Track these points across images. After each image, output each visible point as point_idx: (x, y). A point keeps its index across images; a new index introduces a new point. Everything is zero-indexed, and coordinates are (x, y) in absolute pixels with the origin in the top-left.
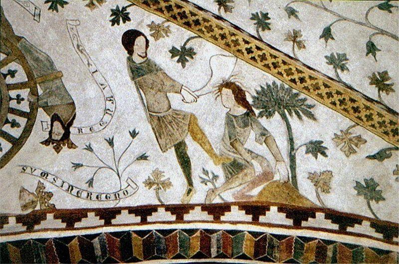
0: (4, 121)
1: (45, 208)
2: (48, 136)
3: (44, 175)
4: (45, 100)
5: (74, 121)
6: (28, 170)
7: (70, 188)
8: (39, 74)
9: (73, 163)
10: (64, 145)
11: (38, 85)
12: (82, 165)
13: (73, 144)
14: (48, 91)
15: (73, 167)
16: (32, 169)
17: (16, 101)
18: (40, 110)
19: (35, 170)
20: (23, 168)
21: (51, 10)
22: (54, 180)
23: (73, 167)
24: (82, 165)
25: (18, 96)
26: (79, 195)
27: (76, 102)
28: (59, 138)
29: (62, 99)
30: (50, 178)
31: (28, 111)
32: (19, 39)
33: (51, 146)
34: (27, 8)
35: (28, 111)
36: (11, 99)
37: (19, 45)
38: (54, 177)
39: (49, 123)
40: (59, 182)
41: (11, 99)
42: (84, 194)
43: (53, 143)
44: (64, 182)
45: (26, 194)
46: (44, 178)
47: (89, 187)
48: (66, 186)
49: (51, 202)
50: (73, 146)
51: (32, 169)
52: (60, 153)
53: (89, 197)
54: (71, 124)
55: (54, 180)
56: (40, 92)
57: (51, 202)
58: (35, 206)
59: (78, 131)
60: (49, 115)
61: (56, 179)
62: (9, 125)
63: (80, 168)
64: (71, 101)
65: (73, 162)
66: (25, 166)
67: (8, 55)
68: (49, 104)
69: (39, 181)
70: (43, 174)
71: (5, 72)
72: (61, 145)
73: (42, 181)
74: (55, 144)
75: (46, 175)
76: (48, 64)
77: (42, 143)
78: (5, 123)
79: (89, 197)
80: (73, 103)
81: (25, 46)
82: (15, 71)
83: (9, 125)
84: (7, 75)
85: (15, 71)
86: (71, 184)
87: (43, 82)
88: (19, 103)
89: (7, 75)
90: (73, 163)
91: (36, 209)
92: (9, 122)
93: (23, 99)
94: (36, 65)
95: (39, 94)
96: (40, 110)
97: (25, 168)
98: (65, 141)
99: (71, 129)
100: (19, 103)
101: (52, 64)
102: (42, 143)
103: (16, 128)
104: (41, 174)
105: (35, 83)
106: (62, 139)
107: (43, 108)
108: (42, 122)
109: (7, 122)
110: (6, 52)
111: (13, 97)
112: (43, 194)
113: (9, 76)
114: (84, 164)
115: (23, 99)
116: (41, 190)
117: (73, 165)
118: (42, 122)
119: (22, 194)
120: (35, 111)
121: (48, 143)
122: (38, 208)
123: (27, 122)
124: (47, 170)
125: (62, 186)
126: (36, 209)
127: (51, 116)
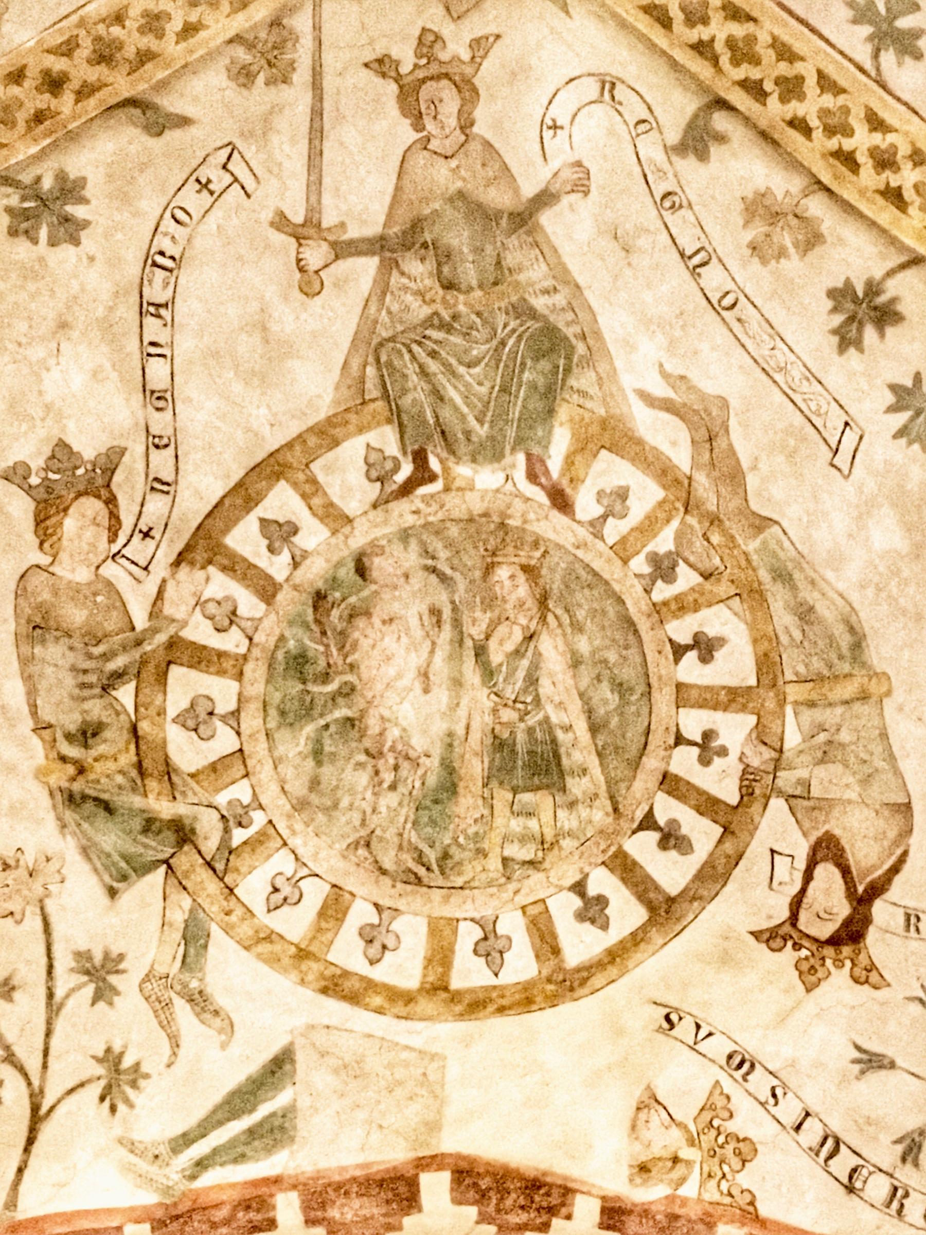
0: (639, 814)
1: (716, 1197)
2: (785, 914)
3: (740, 1066)
4: (803, 773)
5: (898, 880)
6: (685, 1030)
7: (830, 1143)
8: (801, 669)
9: (858, 1048)
10: (839, 964)
11: (789, 710)
12: (892, 1065)
13: (871, 968)
14: (822, 737)
15: (855, 1061)
16: (698, 1027)
17: (695, 751)
18: (777, 805)
19: (710, 1034)
20: (667, 1018)
21: (903, 441)
22: (774, 1095)
23: (855, 1061)
24: (892, 1065)
25: (708, 735)
26: (858, 1185)
27: (917, 807)
28: (825, 931)
29: (866, 781)
30: (760, 1082)
31: (733, 798)
32: (761, 524)
33: (789, 955)
34: (818, 422)
35: (733, 798)
36: (680, 740)
37: (752, 546)
38: (775, 1082)
39: (801, 864)
40: (789, 1111)
41: (680, 740)
42: (878, 1188)
43: (797, 947)
44: (808, 1114)
45: (657, 1117)
46: (738, 1074)
47: (904, 1160)
48: (812, 1132)
49: (744, 1180)
50: (874, 977)
51: (698, 1027)
52: (817, 992)
53: (895, 1205)
54: (876, 890)
55: (774, 1095)
56: (793, 739)
57: (744, 1180)
58: (682, 1181)
59: (901, 920)
60: (805, 834)
61: (779, 1092)
62: (653, 837)
63: (883, 1073)
64: (903, 800)
65: (860, 1042)
66: (677, 1010)
67: (707, 576)
68: (815, 792)
69: (717, 1082)
70: (737, 1060)
71: (685, 638)
72: (829, 962)
73: (728, 1086)
74: (804, 953)
75: (746, 1066)
76: (845, 641)
77: (756, 935)
78: (641, 828)
79: (895, 1205)
80: (908, 806)
81: (775, 555)
82: (721, 641)
83: (653, 837)
84: (688, 648)
85: (721, 641)
86: (836, 1126)
87: (812, 704)
88: (705, 761)
89: (688, 648)
90: (858, 1048)
91: (682, 1192)
92: (658, 828)
93: (723, 752)
94: (797, 635)
95: (786, 746)
96: (777, 805)
97: (674, 1017)
98: (846, 950)
99: (879, 909)
100: (705, 761)
101: (858, 645)
102: (756, 935)
103: (673, 854)
104: (730, 1057)
105: (782, 702)
106: (834, 941)
107: (790, 798)
108: (773, 851)
109: (648, 823)
110: (706, 566)
111: (687, 733)
112: (721, 1139)
113: (692, 655)
114: (899, 1062)
115: (723, 752)
116: (716, 1123)
117: (857, 1055)
118: (773, 851)
119: (643, 1115)
120: (756, 808)
121: (778, 942)
122: (689, 1190)
123: (720, 841)
124: (751, 1045)
125: (798, 1128)
126: (682, 1192)
127: (813, 839)
